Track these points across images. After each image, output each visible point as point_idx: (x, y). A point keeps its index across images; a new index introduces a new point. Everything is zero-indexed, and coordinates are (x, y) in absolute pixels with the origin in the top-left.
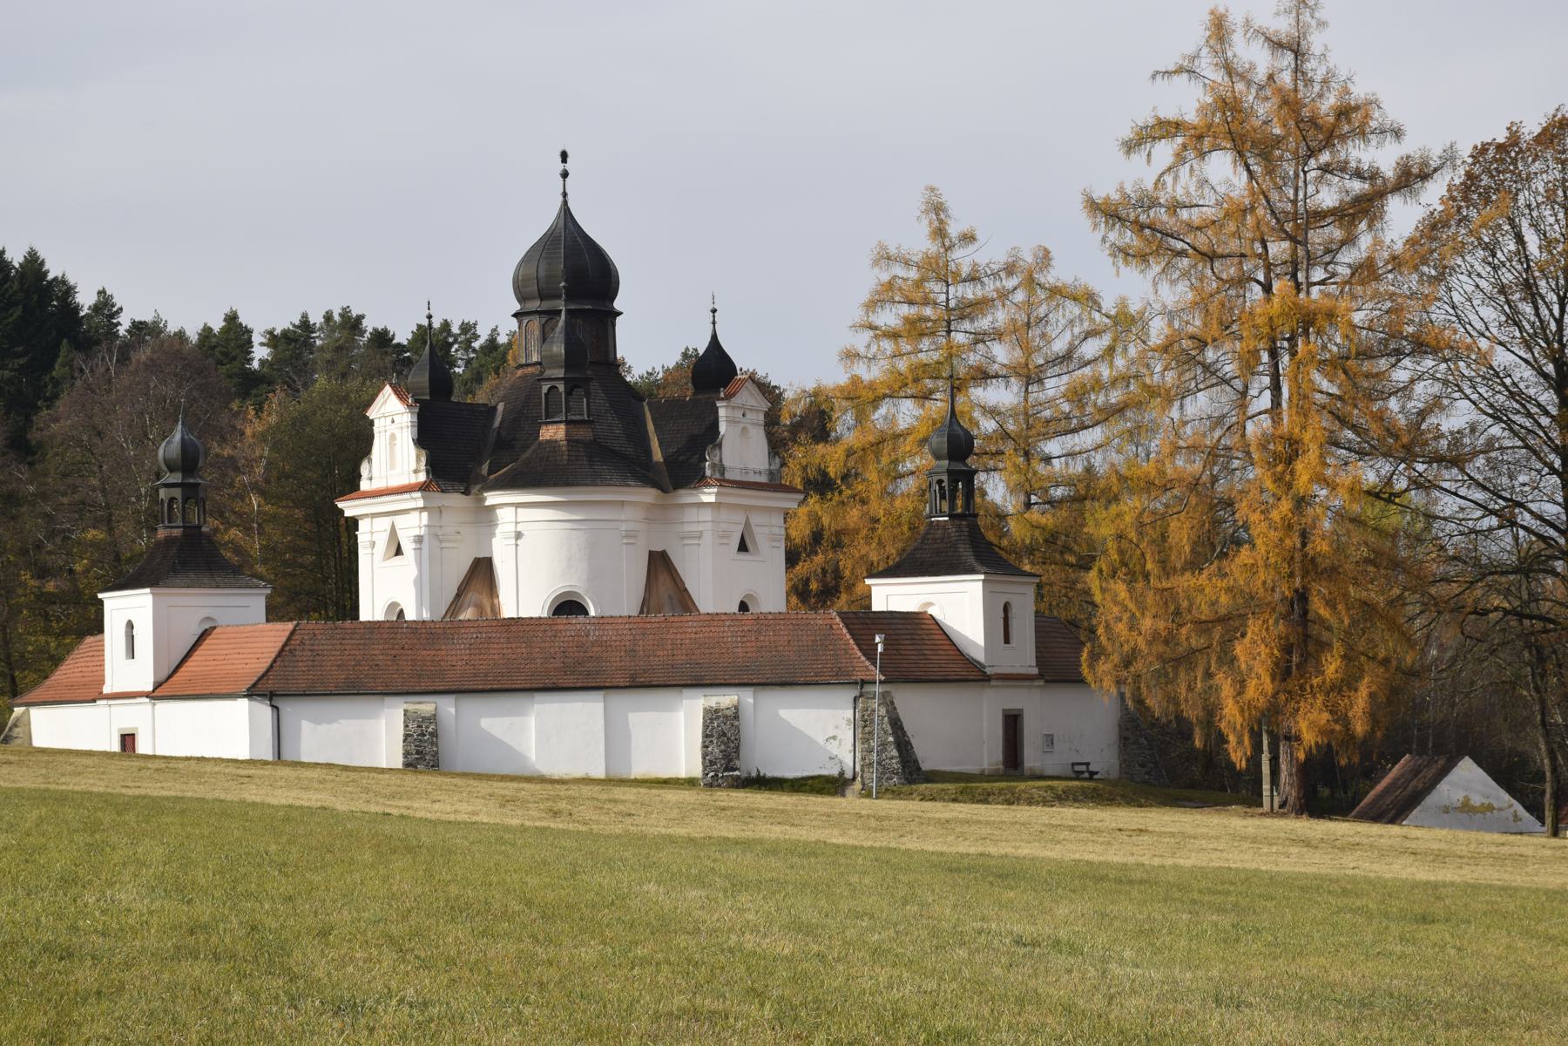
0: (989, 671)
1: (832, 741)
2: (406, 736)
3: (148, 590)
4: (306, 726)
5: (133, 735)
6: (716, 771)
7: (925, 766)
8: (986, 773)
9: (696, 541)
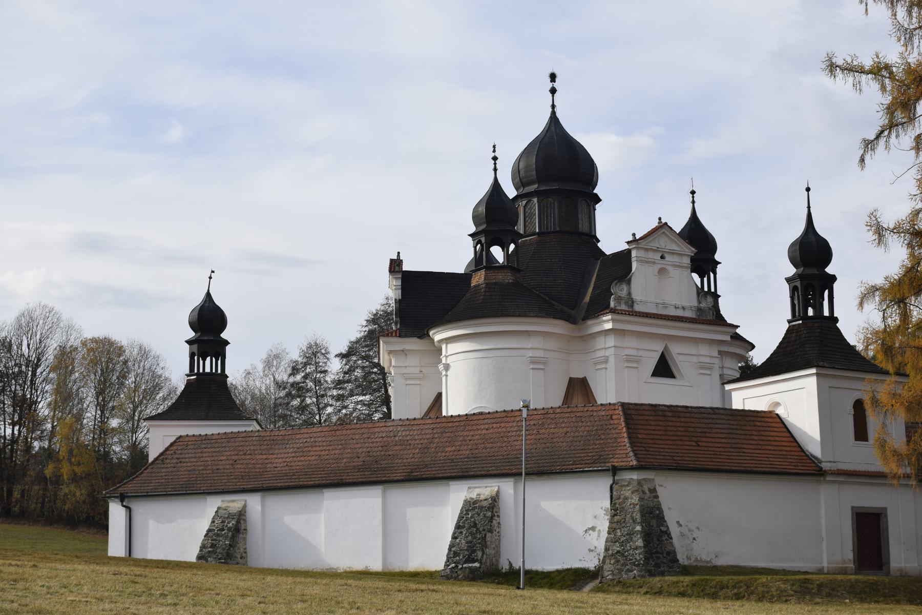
0: (826, 466)
1: (591, 532)
2: (209, 531)
4: (152, 524)
6: (457, 563)
7: (682, 559)
8: (826, 571)
9: (603, 366)
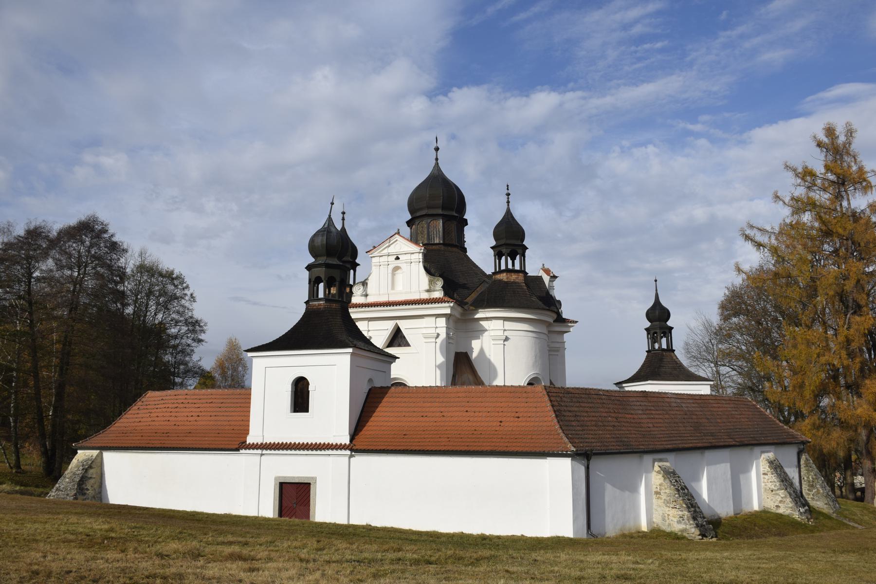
3: (350, 350)
5: (309, 484)
